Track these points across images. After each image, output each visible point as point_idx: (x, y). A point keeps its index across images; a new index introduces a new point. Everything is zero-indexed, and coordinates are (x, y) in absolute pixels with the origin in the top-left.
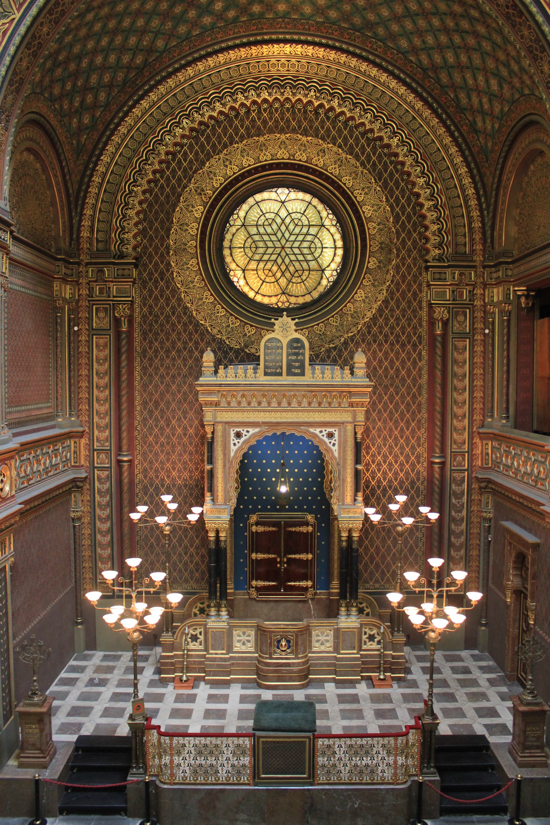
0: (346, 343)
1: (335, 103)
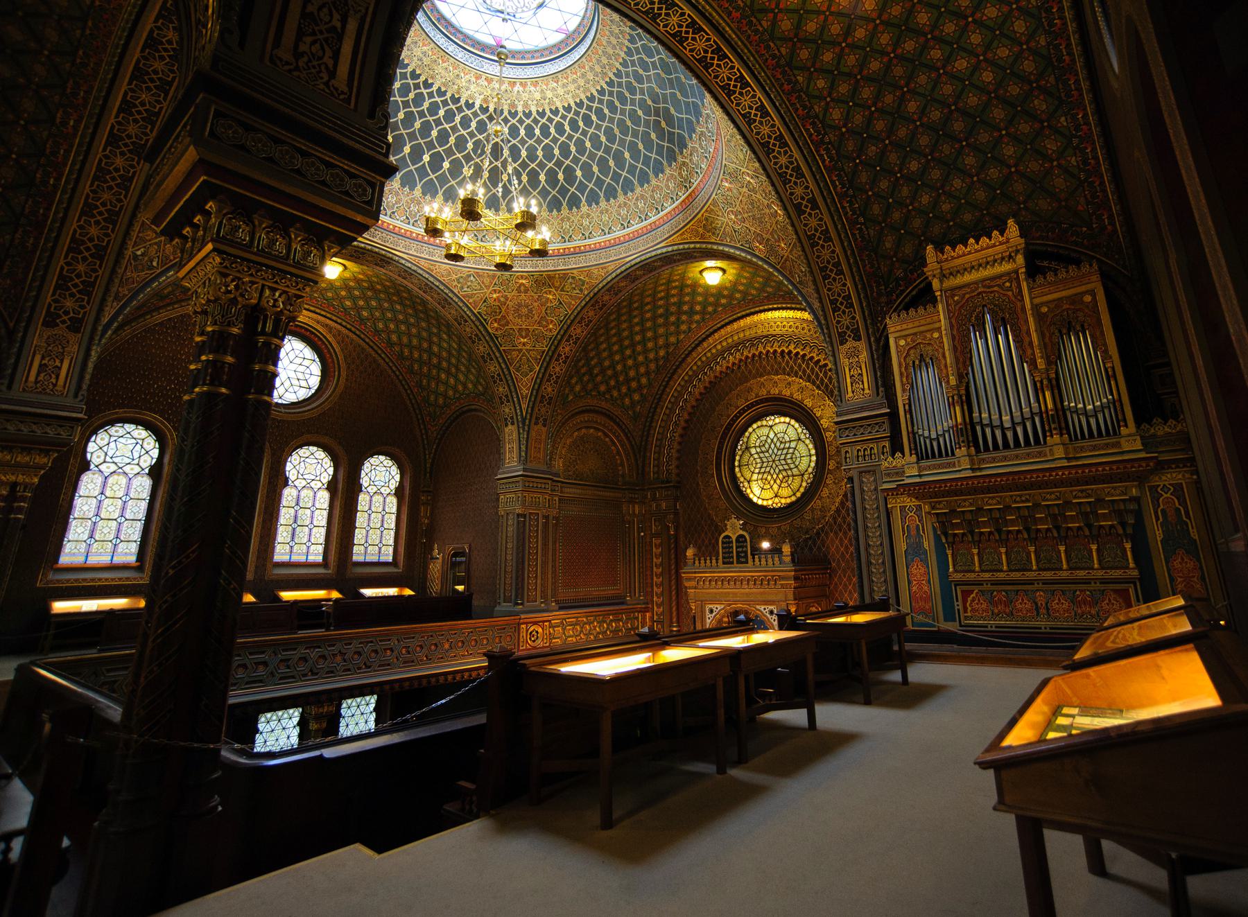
0: (818, 534)
1: (792, 347)
